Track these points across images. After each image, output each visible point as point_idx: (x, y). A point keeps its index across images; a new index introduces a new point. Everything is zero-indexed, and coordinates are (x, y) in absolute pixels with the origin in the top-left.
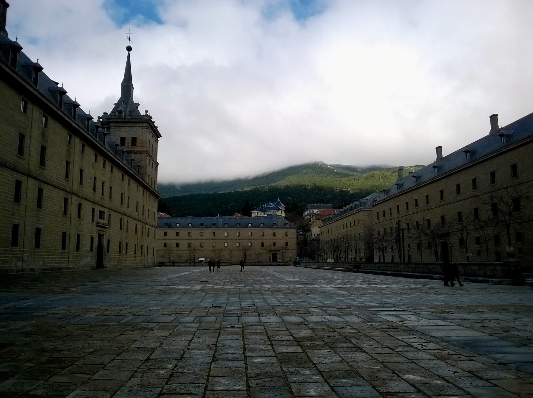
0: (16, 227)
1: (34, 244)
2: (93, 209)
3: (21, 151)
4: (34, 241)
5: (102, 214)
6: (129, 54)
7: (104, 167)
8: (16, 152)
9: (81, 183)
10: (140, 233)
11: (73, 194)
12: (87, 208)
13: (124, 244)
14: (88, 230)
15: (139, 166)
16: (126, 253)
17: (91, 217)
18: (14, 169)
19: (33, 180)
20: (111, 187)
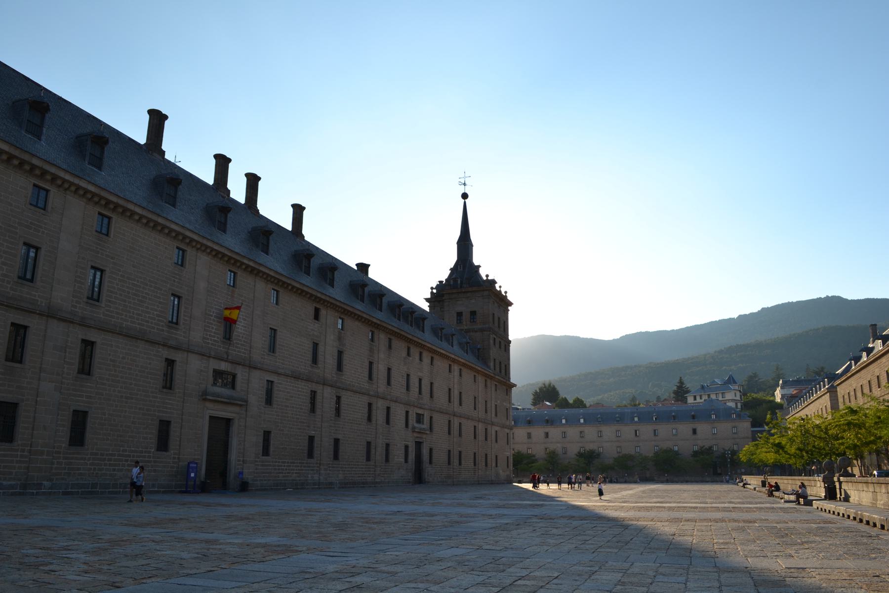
0: (311, 439)
1: (332, 456)
2: (407, 412)
3: (315, 360)
4: (332, 453)
5: (419, 418)
6: (465, 203)
7: (421, 360)
8: (310, 362)
9: (389, 383)
10: (481, 437)
11: (378, 397)
12: (398, 413)
13: (456, 454)
14: (401, 437)
15: (479, 349)
16: (460, 464)
17: (404, 422)
18: (308, 380)
19: (329, 388)
20: (432, 383)
